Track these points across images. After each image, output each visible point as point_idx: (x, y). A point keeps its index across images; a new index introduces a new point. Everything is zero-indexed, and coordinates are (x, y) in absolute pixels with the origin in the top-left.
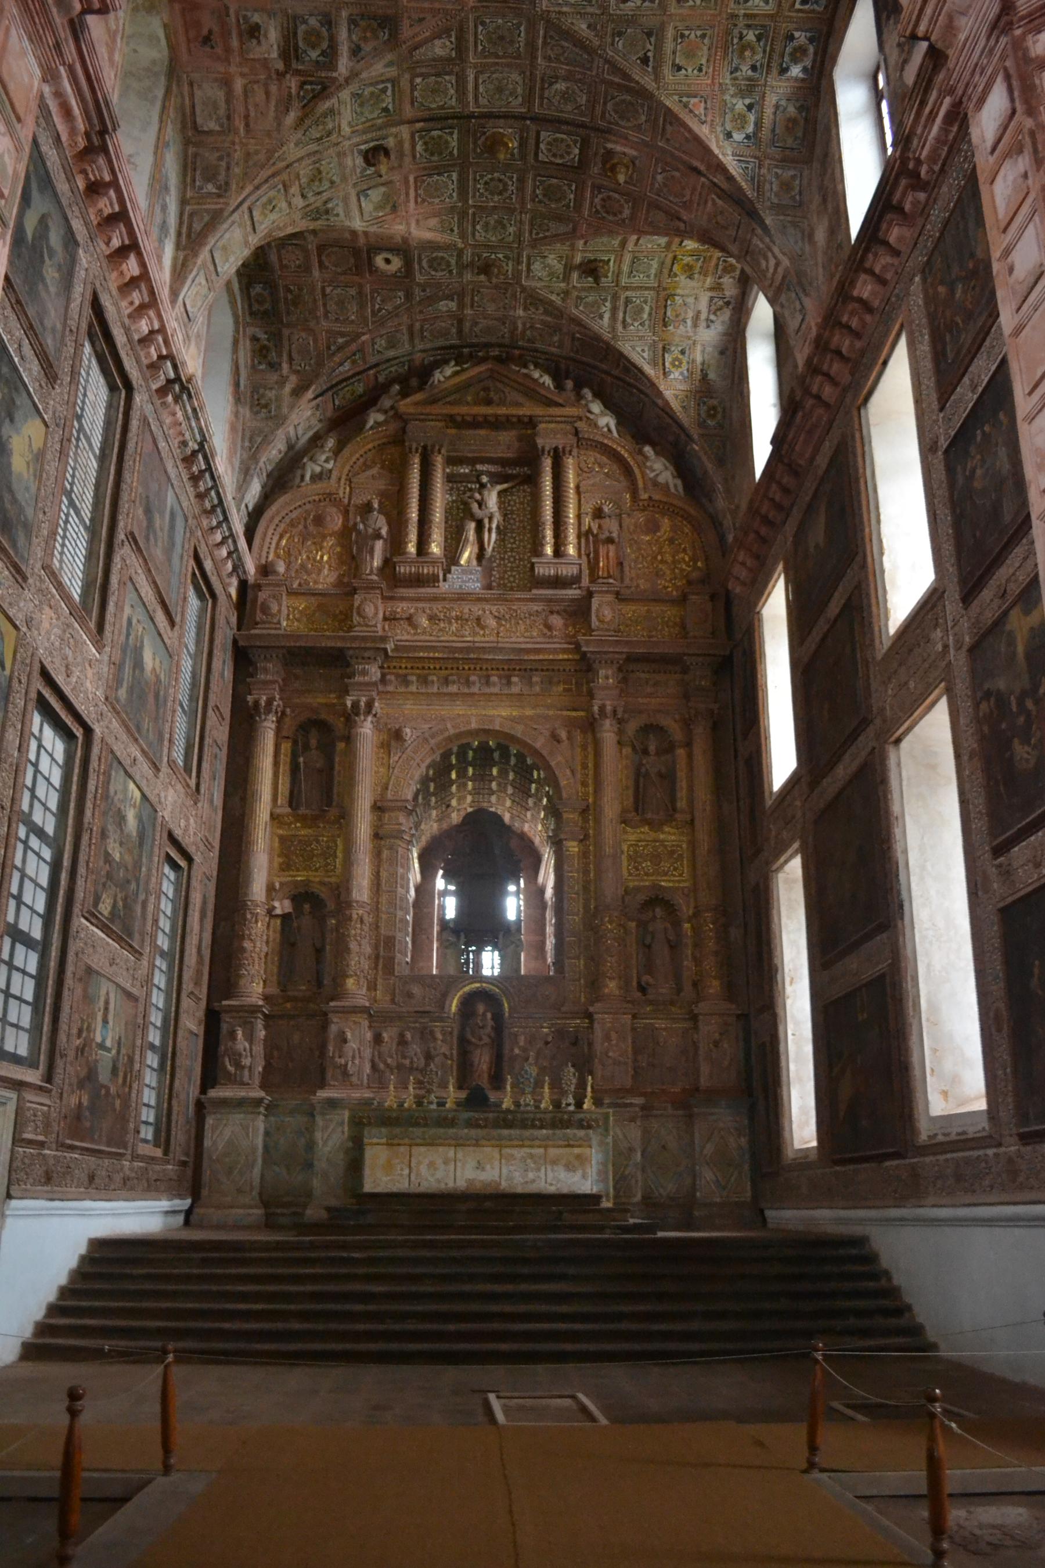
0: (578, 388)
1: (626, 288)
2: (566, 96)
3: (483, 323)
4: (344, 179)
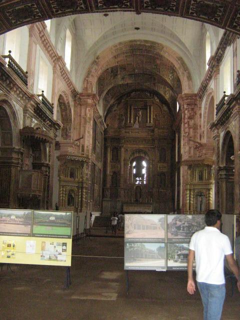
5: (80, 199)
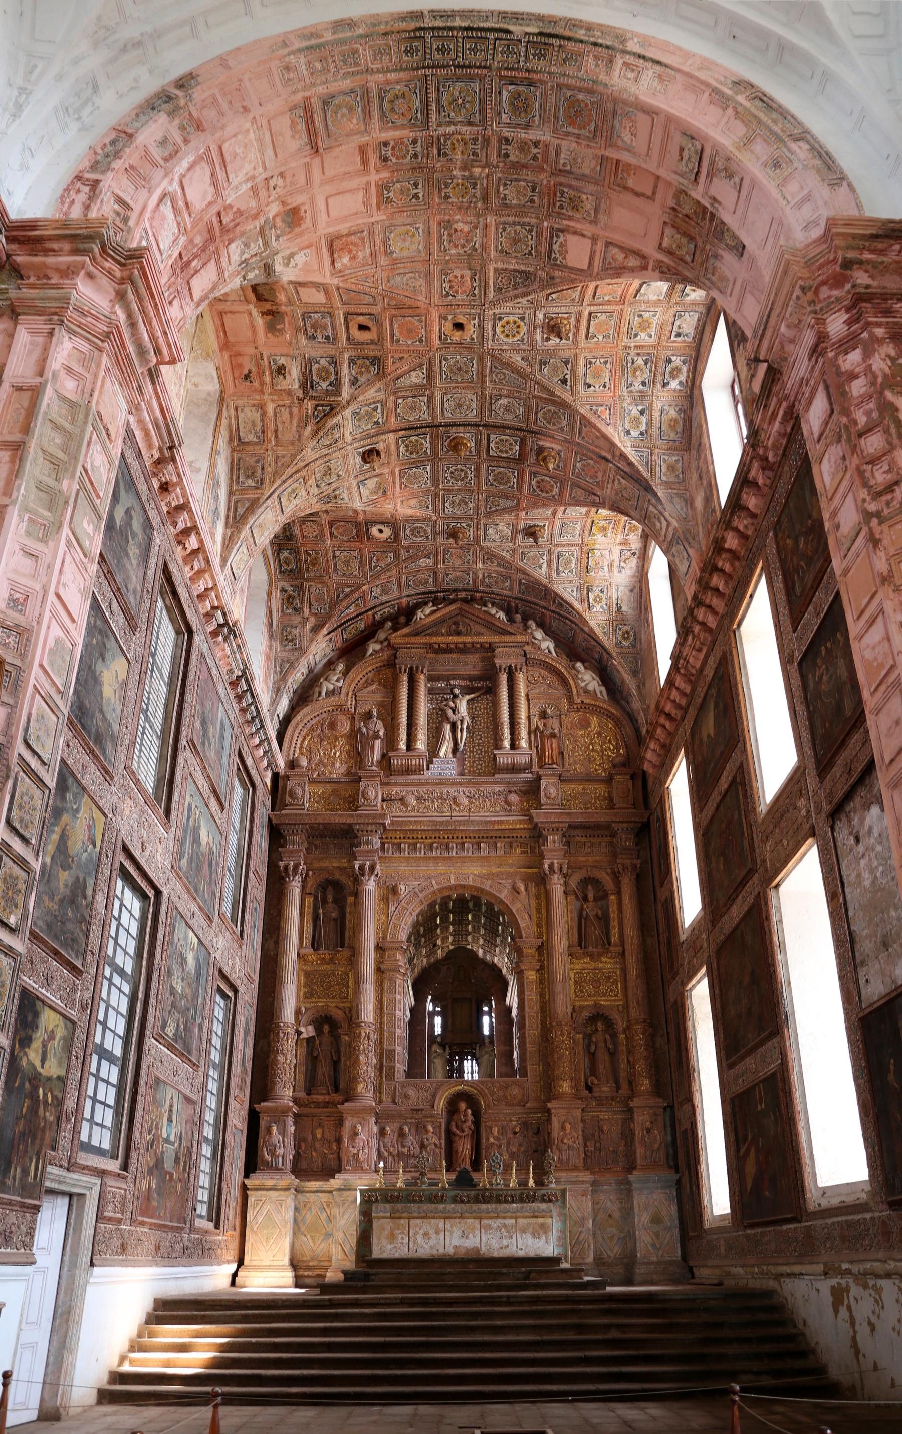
0: (525, 620)
1: (558, 546)
2: (507, 408)
3: (452, 575)
4: (348, 473)
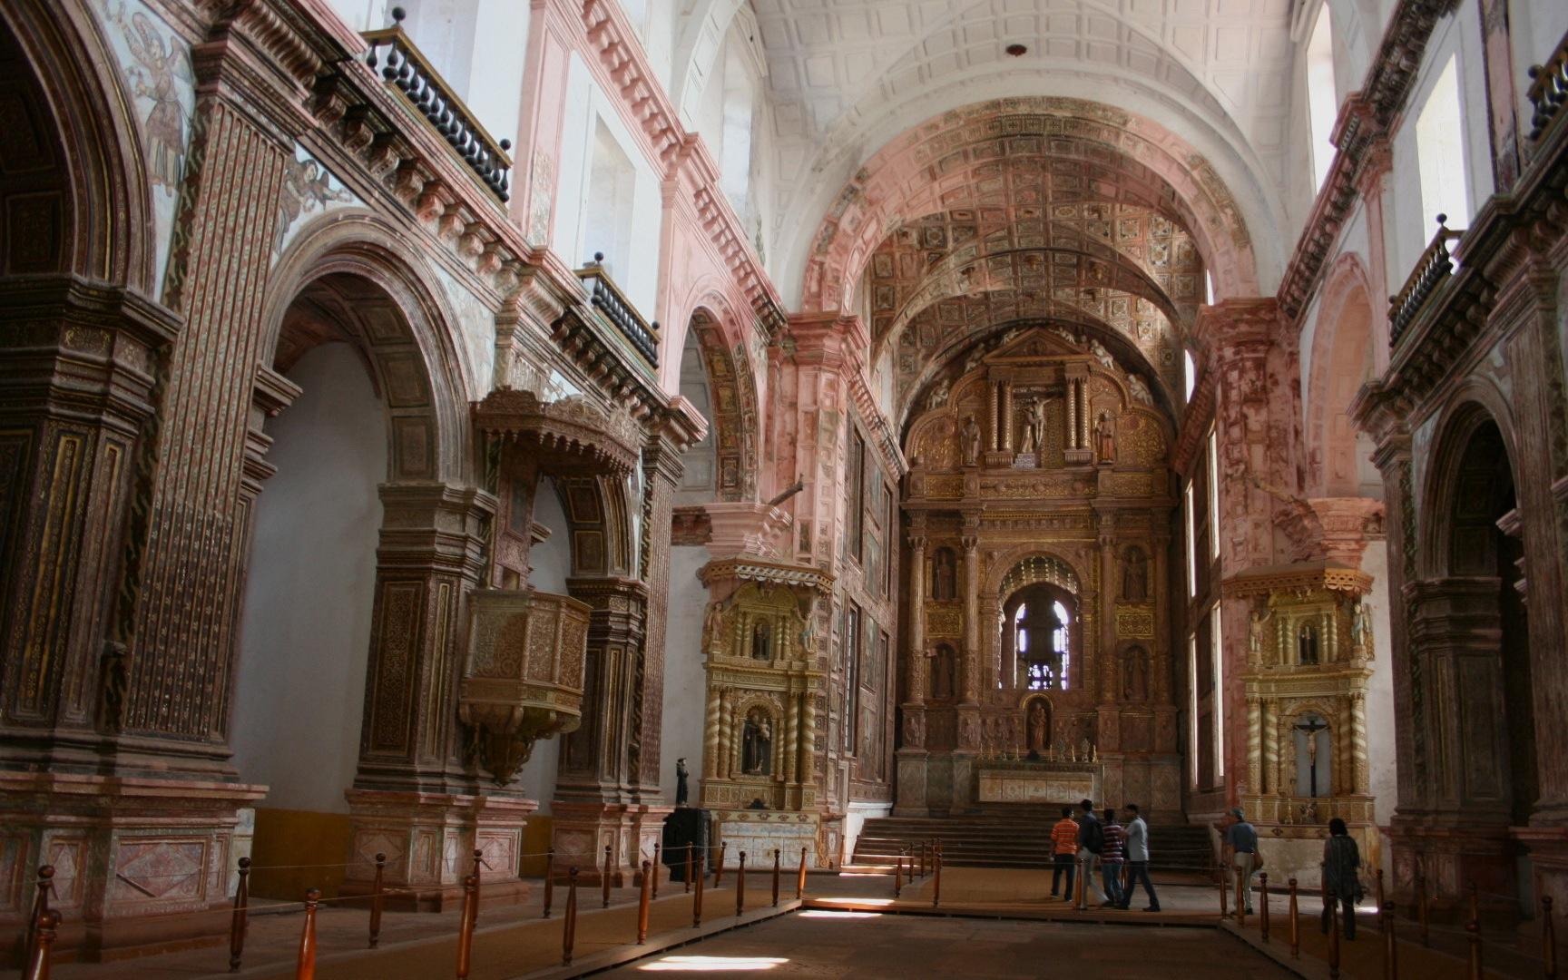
0: (1089, 341)
5: (794, 747)
